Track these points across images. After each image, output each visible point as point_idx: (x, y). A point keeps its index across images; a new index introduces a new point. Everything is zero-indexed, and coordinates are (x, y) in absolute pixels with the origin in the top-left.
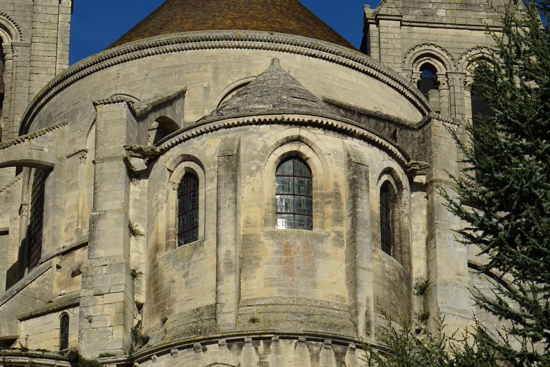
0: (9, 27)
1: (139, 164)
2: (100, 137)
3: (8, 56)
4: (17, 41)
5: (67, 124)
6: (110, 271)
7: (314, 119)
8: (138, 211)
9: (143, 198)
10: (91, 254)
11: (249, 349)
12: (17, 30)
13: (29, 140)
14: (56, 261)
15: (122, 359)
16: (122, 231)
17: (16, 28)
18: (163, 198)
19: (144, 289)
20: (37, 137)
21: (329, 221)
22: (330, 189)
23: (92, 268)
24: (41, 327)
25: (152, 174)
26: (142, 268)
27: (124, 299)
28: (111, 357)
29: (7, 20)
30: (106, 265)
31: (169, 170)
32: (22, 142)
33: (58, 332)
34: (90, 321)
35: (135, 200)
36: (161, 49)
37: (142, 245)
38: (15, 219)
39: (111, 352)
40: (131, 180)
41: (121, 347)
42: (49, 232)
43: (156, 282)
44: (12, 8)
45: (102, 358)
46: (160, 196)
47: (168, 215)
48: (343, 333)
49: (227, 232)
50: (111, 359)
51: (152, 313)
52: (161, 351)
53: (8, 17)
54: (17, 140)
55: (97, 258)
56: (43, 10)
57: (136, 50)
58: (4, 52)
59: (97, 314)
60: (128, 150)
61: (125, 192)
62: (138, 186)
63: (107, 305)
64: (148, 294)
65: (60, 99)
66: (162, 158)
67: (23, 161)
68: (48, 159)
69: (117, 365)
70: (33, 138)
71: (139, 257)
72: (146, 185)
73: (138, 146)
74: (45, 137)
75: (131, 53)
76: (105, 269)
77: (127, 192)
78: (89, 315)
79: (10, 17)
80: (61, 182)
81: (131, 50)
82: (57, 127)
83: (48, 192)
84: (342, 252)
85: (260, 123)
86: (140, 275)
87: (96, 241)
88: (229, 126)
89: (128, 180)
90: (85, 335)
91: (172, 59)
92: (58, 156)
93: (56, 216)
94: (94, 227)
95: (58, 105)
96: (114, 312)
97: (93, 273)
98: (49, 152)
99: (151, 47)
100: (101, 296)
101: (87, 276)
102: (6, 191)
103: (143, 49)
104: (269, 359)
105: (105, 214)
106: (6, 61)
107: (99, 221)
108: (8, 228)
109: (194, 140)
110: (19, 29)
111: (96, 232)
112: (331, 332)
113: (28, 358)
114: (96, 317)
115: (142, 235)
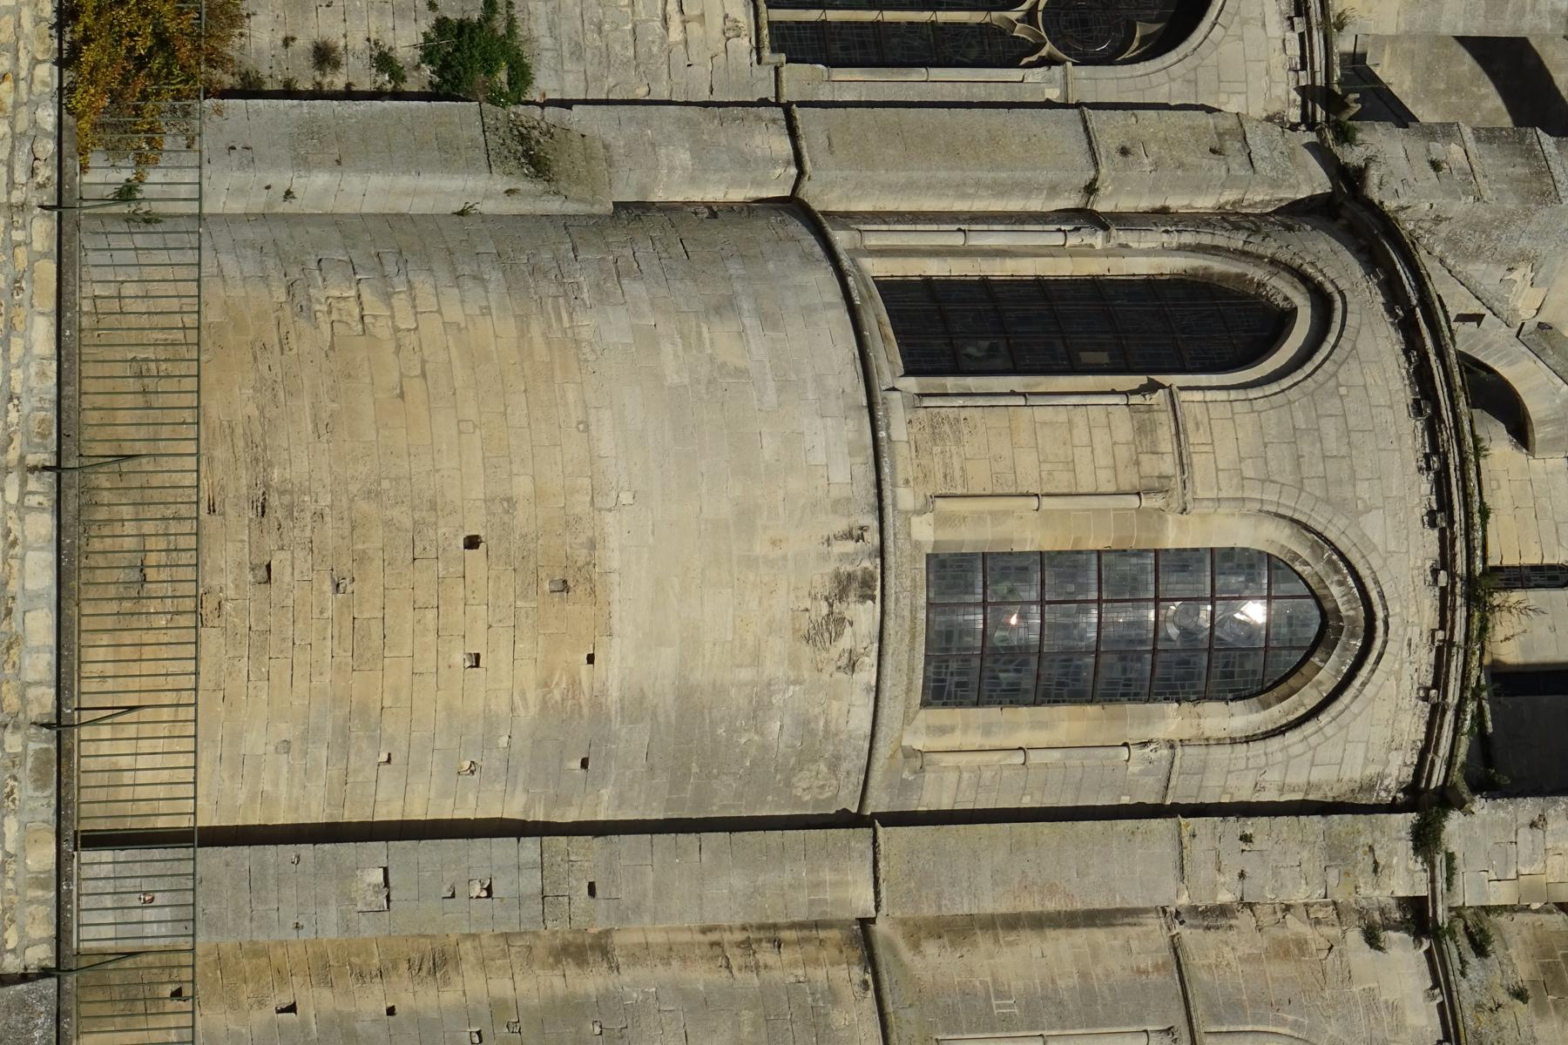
24: (1550, 514)
28: (1445, 886)
33: (1536, 561)
34: (1533, 825)
39: (1458, 880)
50: (1441, 884)
59: (1548, 839)
78: (1549, 821)
113: (1456, 701)
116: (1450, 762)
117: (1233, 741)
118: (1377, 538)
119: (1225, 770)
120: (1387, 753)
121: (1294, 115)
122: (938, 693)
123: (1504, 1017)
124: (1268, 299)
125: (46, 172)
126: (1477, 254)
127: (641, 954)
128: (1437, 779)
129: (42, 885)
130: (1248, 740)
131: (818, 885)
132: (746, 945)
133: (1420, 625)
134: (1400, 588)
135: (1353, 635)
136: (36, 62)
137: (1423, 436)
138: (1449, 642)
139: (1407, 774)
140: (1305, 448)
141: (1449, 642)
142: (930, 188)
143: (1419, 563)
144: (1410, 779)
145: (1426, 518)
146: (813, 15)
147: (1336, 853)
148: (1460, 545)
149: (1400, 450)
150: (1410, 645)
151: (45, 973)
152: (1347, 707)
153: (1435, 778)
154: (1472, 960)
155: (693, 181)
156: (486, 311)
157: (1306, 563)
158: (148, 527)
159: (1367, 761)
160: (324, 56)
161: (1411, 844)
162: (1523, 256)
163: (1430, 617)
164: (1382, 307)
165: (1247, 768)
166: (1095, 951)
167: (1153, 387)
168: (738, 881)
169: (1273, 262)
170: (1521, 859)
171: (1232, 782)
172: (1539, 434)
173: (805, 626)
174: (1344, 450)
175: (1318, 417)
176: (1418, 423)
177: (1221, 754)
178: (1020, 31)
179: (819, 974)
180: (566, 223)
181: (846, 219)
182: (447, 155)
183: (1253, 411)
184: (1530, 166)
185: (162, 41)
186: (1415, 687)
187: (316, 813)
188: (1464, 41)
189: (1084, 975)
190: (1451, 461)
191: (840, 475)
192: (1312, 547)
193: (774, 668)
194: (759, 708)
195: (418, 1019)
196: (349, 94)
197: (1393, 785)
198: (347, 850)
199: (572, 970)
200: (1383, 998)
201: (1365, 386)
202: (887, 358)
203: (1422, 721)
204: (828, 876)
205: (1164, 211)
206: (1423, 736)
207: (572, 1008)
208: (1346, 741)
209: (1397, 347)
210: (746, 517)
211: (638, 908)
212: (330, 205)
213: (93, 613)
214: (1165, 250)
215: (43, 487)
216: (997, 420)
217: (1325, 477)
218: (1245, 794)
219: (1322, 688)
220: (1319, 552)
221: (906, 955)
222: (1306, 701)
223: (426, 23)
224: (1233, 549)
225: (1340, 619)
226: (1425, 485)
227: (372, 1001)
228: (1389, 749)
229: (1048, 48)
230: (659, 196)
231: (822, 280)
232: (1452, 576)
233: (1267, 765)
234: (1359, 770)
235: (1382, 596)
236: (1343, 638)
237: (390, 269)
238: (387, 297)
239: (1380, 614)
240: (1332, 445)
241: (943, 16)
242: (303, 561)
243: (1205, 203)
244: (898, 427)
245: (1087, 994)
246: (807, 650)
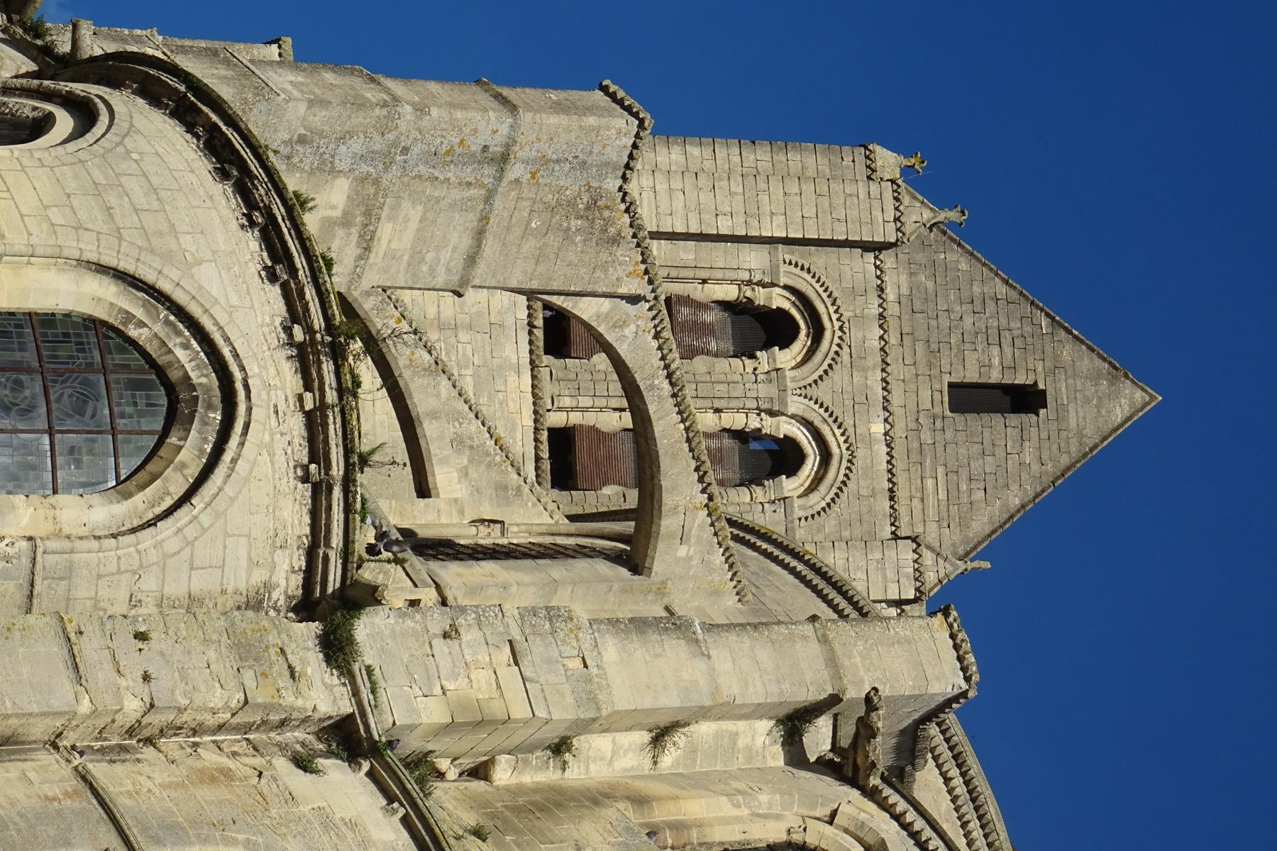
0: (823, 488)
1: (819, 738)
2: (874, 629)
3: (758, 491)
4: (796, 510)
5: (740, 600)
6: (573, 678)
8: (710, 747)
9: (740, 756)
10: (602, 626)
12: (818, 508)
13: (706, 505)
15: (373, 725)
16: (669, 701)
17: (823, 504)
18: (760, 806)
19: (529, 778)
20: (712, 524)
23: (571, 630)
26: (575, 767)
27: (517, 721)
28: (371, 697)
29: (838, 484)
30: (586, 666)
31: (834, 814)
32: (700, 487)
35: (734, 736)
36: (968, 808)
37: (631, 765)
38: (461, 512)
40: (780, 721)
41: (397, 723)
42: (493, 576)
43: (558, 805)
44: (864, 492)
45: (364, 672)
46: (764, 798)
47: (725, 821)
50: (365, 694)
52: (420, 826)
53: (846, 485)
54: (706, 473)
55: (596, 642)
56: (875, 564)
57: (951, 749)
58: (766, 483)
59: (465, 651)
60: (868, 699)
61: (759, 705)
62: (767, 742)
63: (493, 676)
64: (519, 790)
65: (786, 583)
66: (855, 794)
67: (656, 495)
69: (353, 714)
70: (709, 515)
71: (602, 759)
72: (771, 763)
73: (880, 724)
74: (711, 546)
75: (942, 737)
76: (576, 664)
77: (757, 712)
78: (461, 631)
79: (844, 488)
80: (611, 594)
81: (948, 735)
82: (735, 574)
86: (559, 764)
87: (635, 639)
89: (782, 712)
90: (409, 623)
92: (669, 583)
93: (532, 589)
94: (667, 629)
95: (770, 578)
96: (481, 697)
97: (562, 634)
98: (678, 560)
99: (967, 783)
100: (511, 660)
101: (550, 620)
102: (520, 486)
103: (959, 766)
105: (703, 654)
106: (746, 490)
107: (683, 642)
108: (438, 496)
110: (822, 513)
111: (655, 637)
113: (341, 473)
114: (458, 648)
115: (655, 763)
118: (215, 291)
119: (94, 573)
120: (272, 553)
124: (13, 115)
128: (334, 580)
133: (283, 388)
134: (253, 346)
135: (210, 407)
137: (236, 198)
138: (322, 406)
140: (112, 200)
141: (322, 406)
143: (268, 320)
144: (300, 592)
145: (263, 273)
148: (310, 293)
149: (216, 208)
150: (276, 412)
152: (220, 490)
153: (331, 578)
157: (141, 324)
159: (253, 564)
161: (321, 655)
163: (291, 379)
164: (147, 106)
165: (119, 572)
170: (443, 673)
171: (104, 593)
174: (155, 205)
175: (117, 175)
176: (226, 187)
183: (43, 166)
184: (233, 70)
186: (292, 464)
190: (276, 211)
192: (144, 306)
197: (281, 602)
200: (338, 816)
201: (157, 153)
203: (305, 510)
206: (307, 530)
208: (226, 535)
209: (178, 129)
217: (143, 228)
219: (186, 472)
220: (154, 311)
222: (172, 489)
224: (53, 314)
225: (192, 387)
228: (274, 548)
232: (309, 330)
233: (141, 566)
234: (244, 576)
235: (236, 356)
236: (200, 409)
239: (238, 376)
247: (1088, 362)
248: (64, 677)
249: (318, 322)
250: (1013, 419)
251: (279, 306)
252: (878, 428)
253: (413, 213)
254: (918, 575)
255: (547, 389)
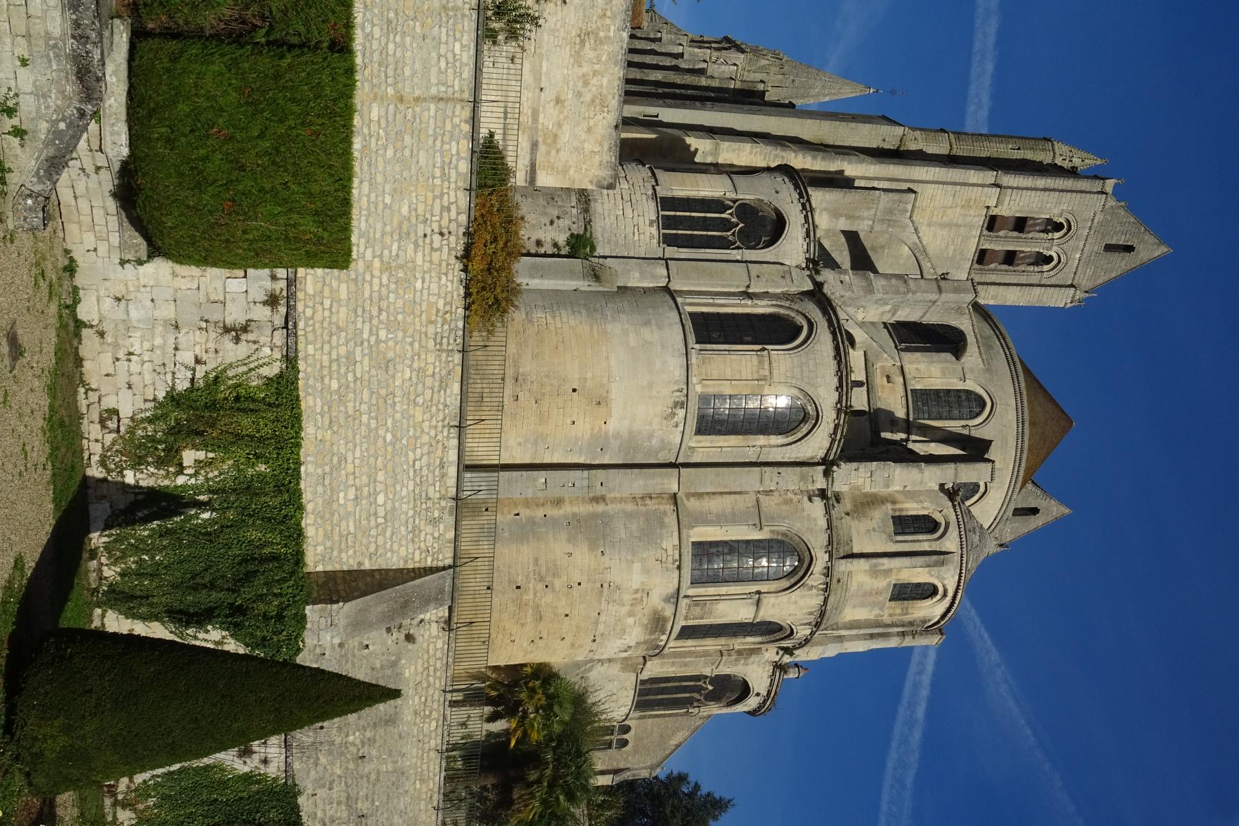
7: (956, 605)
11: (823, 579)
14: (899, 364)
21: (891, 611)
22: (910, 611)
25: (942, 495)
47: (913, 509)
48: (823, 627)
49: (897, 562)
51: (854, 500)
66: (950, 504)
68: (963, 360)
83: (944, 355)
84: (872, 617)
85: (960, 576)
88: (962, 557)
91: (1012, 442)
104: (814, 591)
109: (957, 533)
112: (824, 622)
116: (835, 454)
117: (778, 446)
121: (804, 265)
122: (700, 431)
123: (843, 521)
125: (459, 340)
126: (849, 306)
127: (614, 500)
128: (831, 458)
129: (450, 542)
130: (782, 446)
131: (663, 484)
132: (642, 498)
136: (457, 308)
139: (823, 455)
142: (704, 285)
146: (674, 232)
147: (803, 478)
148: (844, 397)
151: (450, 567)
154: (836, 504)
155: (639, 281)
156: (581, 323)
158: (484, 386)
160: (539, 243)
162: (862, 306)
163: (834, 416)
166: (736, 501)
167: (764, 349)
168: (641, 482)
169: (797, 311)
172: (857, 346)
173: (665, 415)
177: (773, 449)
178: (731, 238)
179: (662, 507)
180: (604, 294)
181: (681, 293)
182: (572, 275)
185: (496, 299)
187: (527, 461)
188: (843, 232)
189: (733, 508)
191: (677, 373)
193: (655, 426)
194: (651, 436)
195: (552, 518)
196: (545, 255)
198: (535, 473)
199: (595, 505)
202: (691, 338)
204: (666, 481)
205: (767, 292)
207: (594, 516)
210: (651, 385)
211: (614, 489)
212: (539, 287)
213: (470, 408)
214: (768, 306)
215: (454, 432)
216: (720, 358)
218: (779, 459)
221: (686, 502)
223: (568, 234)
226: (836, 380)
227: (540, 513)
229: (738, 243)
230: (629, 285)
231: (674, 315)
237: (555, 309)
238: (554, 317)
240: (811, 367)
241: (710, 233)
242: (527, 395)
243: (779, 291)
244: (694, 359)
245: (734, 514)
246: (665, 421)
247: (1152, 240)
248: (758, 484)
249: (844, 404)
250: (1122, 254)
251: (837, 397)
252: (1078, 256)
253: (907, 310)
254: (1073, 297)
255: (982, 241)
